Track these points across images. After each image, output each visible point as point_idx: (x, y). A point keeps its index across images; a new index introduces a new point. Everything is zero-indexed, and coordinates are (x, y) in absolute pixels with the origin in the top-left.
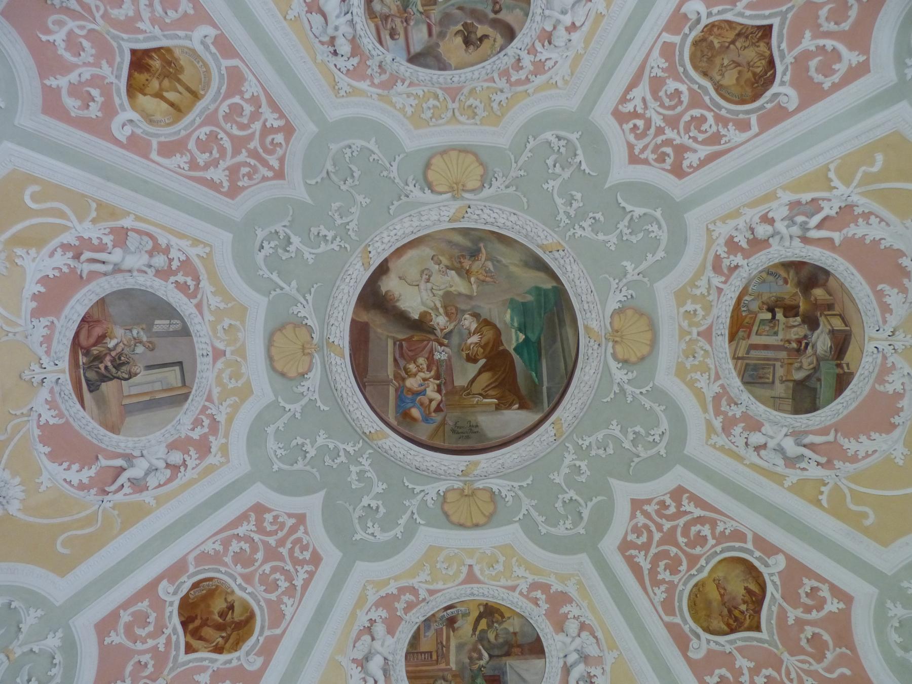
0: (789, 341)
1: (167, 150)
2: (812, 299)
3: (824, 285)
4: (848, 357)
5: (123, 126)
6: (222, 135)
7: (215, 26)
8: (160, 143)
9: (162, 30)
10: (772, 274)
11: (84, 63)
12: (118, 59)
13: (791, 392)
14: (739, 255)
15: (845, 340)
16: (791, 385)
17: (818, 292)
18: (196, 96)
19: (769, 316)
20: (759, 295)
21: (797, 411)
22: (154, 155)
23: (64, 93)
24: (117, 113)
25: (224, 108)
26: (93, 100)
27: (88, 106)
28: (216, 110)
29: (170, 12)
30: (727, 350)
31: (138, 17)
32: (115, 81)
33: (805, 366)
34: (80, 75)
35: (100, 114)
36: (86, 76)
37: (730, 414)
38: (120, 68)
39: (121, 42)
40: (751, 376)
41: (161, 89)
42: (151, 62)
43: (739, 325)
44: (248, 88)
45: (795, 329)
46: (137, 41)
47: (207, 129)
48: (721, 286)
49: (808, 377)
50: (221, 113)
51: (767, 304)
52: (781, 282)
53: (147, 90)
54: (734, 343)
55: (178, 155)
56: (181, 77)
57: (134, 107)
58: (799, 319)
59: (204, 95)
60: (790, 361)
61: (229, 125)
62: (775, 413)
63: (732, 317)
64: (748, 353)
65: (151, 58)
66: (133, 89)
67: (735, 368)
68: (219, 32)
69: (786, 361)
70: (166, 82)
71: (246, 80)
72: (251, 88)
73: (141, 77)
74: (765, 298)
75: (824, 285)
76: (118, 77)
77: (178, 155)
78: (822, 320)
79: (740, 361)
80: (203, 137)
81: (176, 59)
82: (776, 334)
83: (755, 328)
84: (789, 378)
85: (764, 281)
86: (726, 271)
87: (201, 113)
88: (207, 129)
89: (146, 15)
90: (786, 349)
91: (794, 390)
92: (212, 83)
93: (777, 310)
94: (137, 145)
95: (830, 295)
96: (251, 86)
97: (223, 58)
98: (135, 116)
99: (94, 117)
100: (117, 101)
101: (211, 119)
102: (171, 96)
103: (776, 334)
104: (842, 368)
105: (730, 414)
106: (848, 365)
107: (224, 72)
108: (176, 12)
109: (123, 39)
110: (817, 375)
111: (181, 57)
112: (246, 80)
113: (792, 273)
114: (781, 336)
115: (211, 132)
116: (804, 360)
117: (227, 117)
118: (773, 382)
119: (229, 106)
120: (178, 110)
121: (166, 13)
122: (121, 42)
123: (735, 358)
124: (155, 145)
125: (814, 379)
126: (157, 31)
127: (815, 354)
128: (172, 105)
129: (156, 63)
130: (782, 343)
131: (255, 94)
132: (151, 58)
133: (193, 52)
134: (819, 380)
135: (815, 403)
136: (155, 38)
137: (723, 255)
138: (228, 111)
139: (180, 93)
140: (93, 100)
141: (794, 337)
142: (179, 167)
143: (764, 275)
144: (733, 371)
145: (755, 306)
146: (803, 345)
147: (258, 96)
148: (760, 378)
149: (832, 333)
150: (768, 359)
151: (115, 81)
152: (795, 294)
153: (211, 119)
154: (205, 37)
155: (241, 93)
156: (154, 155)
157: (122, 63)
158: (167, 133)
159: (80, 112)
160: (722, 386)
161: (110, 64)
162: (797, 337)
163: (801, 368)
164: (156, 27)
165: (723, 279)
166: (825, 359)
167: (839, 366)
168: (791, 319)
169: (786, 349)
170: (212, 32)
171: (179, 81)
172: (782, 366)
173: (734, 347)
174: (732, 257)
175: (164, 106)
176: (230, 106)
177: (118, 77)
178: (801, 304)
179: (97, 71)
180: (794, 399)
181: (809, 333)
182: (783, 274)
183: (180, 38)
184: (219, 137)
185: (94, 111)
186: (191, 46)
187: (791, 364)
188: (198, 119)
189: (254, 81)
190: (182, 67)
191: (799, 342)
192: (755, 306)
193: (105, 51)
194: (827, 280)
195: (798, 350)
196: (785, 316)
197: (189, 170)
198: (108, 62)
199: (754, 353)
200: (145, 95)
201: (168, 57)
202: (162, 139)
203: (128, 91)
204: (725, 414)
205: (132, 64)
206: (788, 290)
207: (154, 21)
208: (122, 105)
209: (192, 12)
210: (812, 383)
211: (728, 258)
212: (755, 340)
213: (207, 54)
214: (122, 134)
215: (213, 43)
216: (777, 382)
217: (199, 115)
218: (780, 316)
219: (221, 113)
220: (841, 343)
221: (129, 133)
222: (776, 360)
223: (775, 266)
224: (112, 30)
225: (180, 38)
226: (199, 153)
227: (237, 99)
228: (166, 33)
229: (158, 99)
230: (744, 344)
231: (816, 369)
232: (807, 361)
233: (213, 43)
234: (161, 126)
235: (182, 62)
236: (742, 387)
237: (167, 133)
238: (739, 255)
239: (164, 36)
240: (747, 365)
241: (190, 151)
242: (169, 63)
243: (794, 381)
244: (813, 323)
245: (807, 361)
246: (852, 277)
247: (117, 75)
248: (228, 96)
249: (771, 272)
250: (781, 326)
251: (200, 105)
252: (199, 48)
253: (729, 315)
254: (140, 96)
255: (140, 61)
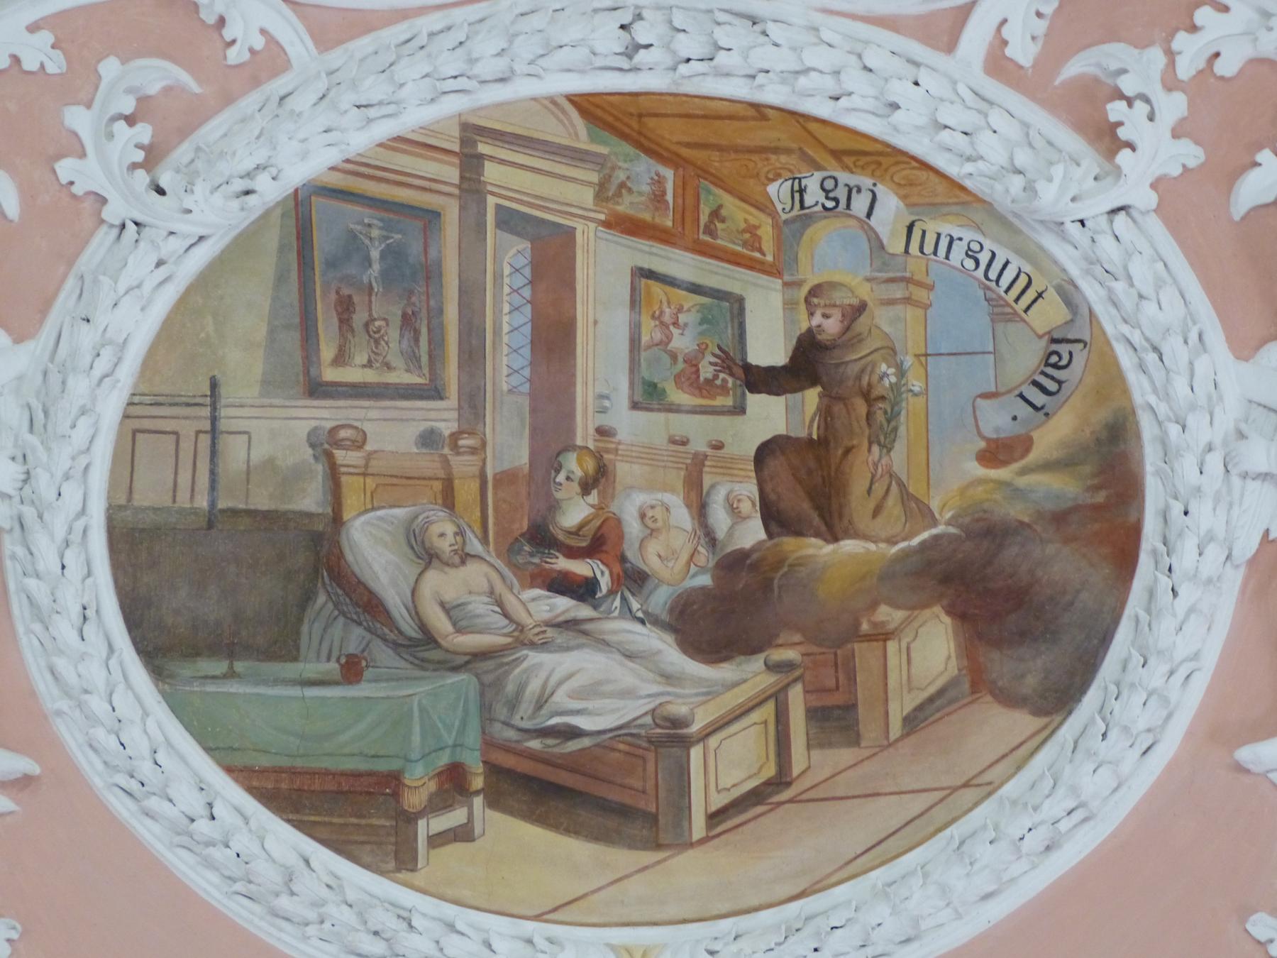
0: (598, 479)
2: (888, 615)
3: (976, 681)
4: (509, 835)
10: (1052, 363)
13: (262, 502)
14: (1191, 154)
15: (625, 812)
16: (311, 499)
17: (930, 648)
19: (768, 346)
20: (910, 288)
21: (136, 545)
30: (523, 88)
33: (442, 585)
37: (79, 119)
40: (353, 246)
43: (694, 161)
45: (682, 517)
48: (975, 38)
49: (369, 606)
51: (849, 336)
52: (997, 420)
54: (578, 133)
58: (752, 533)
60: (466, 491)
62: (111, 407)
63: (759, 111)
64: (509, 221)
67: (400, 143)
69: (463, 465)
74: (883, 319)
75: (976, 681)
78: (748, 675)
79: (451, 173)
82: (648, 396)
83: (680, 263)
84: (350, 484)
85: (1001, 313)
86: (1077, 67)
90: (548, 456)
91: (268, 519)
93: (812, 396)
95: (913, 722)
103: (648, 396)
104: (439, 803)
105: (79, 119)
106: (463, 834)
110: (384, 655)
113: (1063, 488)
114: (632, 426)
116: (475, 574)
118: (317, 389)
123: (472, 143)
125: (355, 638)
127: (523, 639)
130: (584, 434)
134: (352, 670)
135: (193, 652)
137: (1190, 52)
141: (629, 508)
143: (1049, 315)
144: (384, 130)
145: (831, 255)
146: (581, 568)
148: (345, 308)
149: (670, 738)
150: (473, 356)
152: (918, 511)
160: (271, 60)
162: (633, 528)
163: (428, 557)
165: (1022, 51)
166: (489, 701)
167: (453, 782)
168: (749, 489)
169: (548, 456)
172: (429, 439)
173: (552, 131)
174: (1173, 107)
178: (849, 546)
180: (212, 519)
181: (660, 599)
182: (1053, 436)
187: (448, 499)
191: (600, 540)
192: (831, 255)
194: (1010, 699)
195: (541, 537)
196: (765, 452)
199: (510, 258)
204: (78, 84)
206: (941, 467)
210: (326, 630)
211: (1171, 83)
212: (604, 266)
216: (325, 414)
218: (770, 416)
220: (595, 792)
222: (473, 404)
223: (1111, 381)
230: (568, 194)
231: (421, 648)
232: (472, 592)
236: (270, 191)
238: (1191, 154)
240: (431, 217)
243: (337, 520)
244: (721, 620)
245: (472, 592)
246: (1033, 842)
249: (1069, 354)
250: (699, 431)
253: (773, 94)
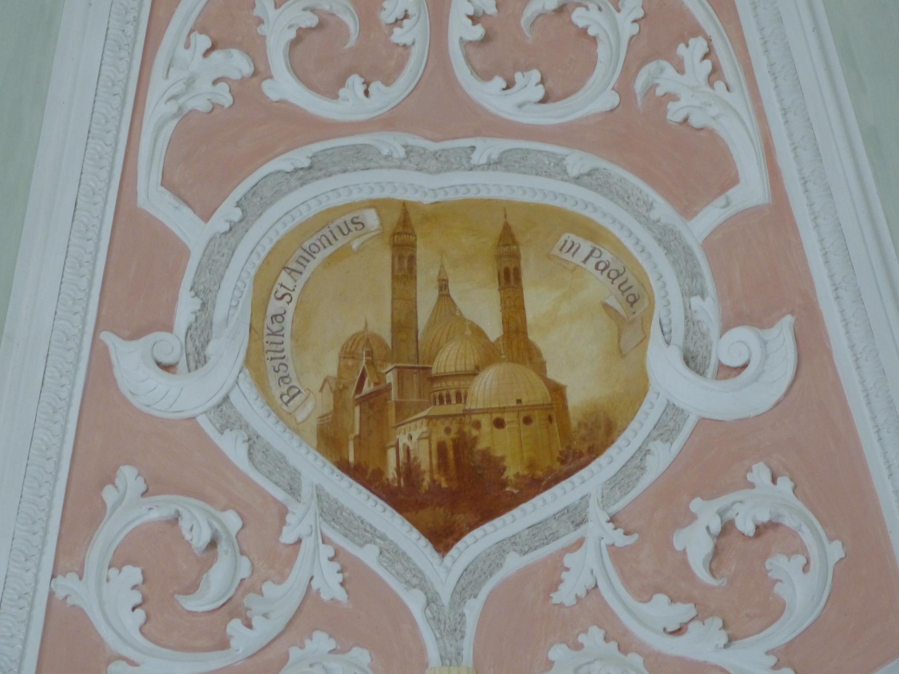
1: (688, 164)
5: (728, 372)
6: (461, 29)
7: (100, 368)
8: (688, 211)
9: (283, 512)
11: (623, 649)
12: (514, 563)
18: (403, 232)
22: (751, 190)
23: (781, 633)
24: (703, 422)
25: (352, 103)
26: (728, 528)
27: (760, 530)
28: (388, 122)
29: (200, 538)
31: (311, 612)
32: (597, 517)
34: (679, 631)
35: (760, 474)
36: (662, 610)
38: (540, 533)
39: (445, 599)
41: (490, 355)
42: (425, 459)
44: (204, 86)
46: (392, 554)
47: (489, 95)
50: (385, 97)
53: (540, 395)
55: (675, 113)
56: (383, 329)
57: (637, 390)
59: (374, 204)
61: (399, 36)
65: (409, 471)
66: (572, 441)
68: (106, 337)
70: (449, 359)
71: (186, 118)
72: (195, 75)
73: (508, 448)
76: (575, 516)
77: (675, 113)
80: (530, 86)
81: (339, 393)
87: (445, 163)
88: (489, 95)
89: (280, 599)
92: (306, 214)
94: (764, 274)
96: (190, 82)
97: (184, 252)
98: (663, 365)
99: (785, 484)
100: (662, 457)
101: (440, 112)
102: (482, 308)
107: (228, 212)
108: (175, 520)
109: (432, 600)
111: (315, 383)
112: (186, 118)
115: (485, 76)
117: (378, 66)
119: (335, 96)
120: (508, 248)
121: (213, 544)
122: (445, 599)
124: (711, 217)
126: (300, 523)
128: (510, 279)
129: (414, 440)
131: (203, 42)
132: (409, 471)
133: (261, 359)
136: (331, 511)
138: (356, 82)
139: (443, 285)
140: (728, 528)
142: (715, 73)
147: (200, 27)
151: (597, 517)
153: (440, 112)
154: (168, 368)
155: (245, 91)
156: (751, 190)
157: (513, 541)
158: (631, 215)
159: (807, 537)
161: (552, 574)
164: (288, 536)
170: (131, 363)
171: (403, 325)
175: (537, 301)
176: (331, 92)
177: (575, 516)
179: (616, 596)
183: (252, 441)
184: (477, 32)
185: (762, 497)
186: (246, 384)
188: (478, 158)
189: (158, 86)
190: (348, 353)
193: (527, 619)
197: (697, 31)
198: (555, 586)
200: (557, 391)
201: (355, 418)
202: (663, 210)
203: (594, 452)
205: (489, 511)
207: (279, 560)
208: (664, 430)
209: (128, 475)
213: (219, 315)
214: (767, 358)
215: (169, 328)
217: (463, 161)
219: (385, 97)
221: (743, 334)
224: (433, 654)
225: (252, 441)
226: (602, 51)
227: (284, 87)
228: (280, 495)
229: (532, 337)
233: (169, 328)
234: (618, 248)
235: (331, 367)
237: (631, 215)
239: (294, 491)
241: (624, 88)
242: (374, 403)
247: (569, 530)
248: (302, 127)
251: (421, 188)
252: (228, 351)
254: (576, 399)
255: (455, 495)
